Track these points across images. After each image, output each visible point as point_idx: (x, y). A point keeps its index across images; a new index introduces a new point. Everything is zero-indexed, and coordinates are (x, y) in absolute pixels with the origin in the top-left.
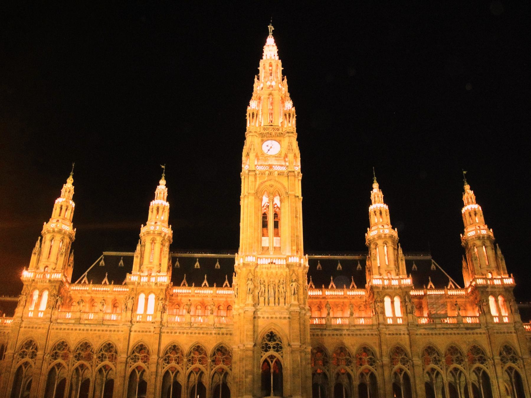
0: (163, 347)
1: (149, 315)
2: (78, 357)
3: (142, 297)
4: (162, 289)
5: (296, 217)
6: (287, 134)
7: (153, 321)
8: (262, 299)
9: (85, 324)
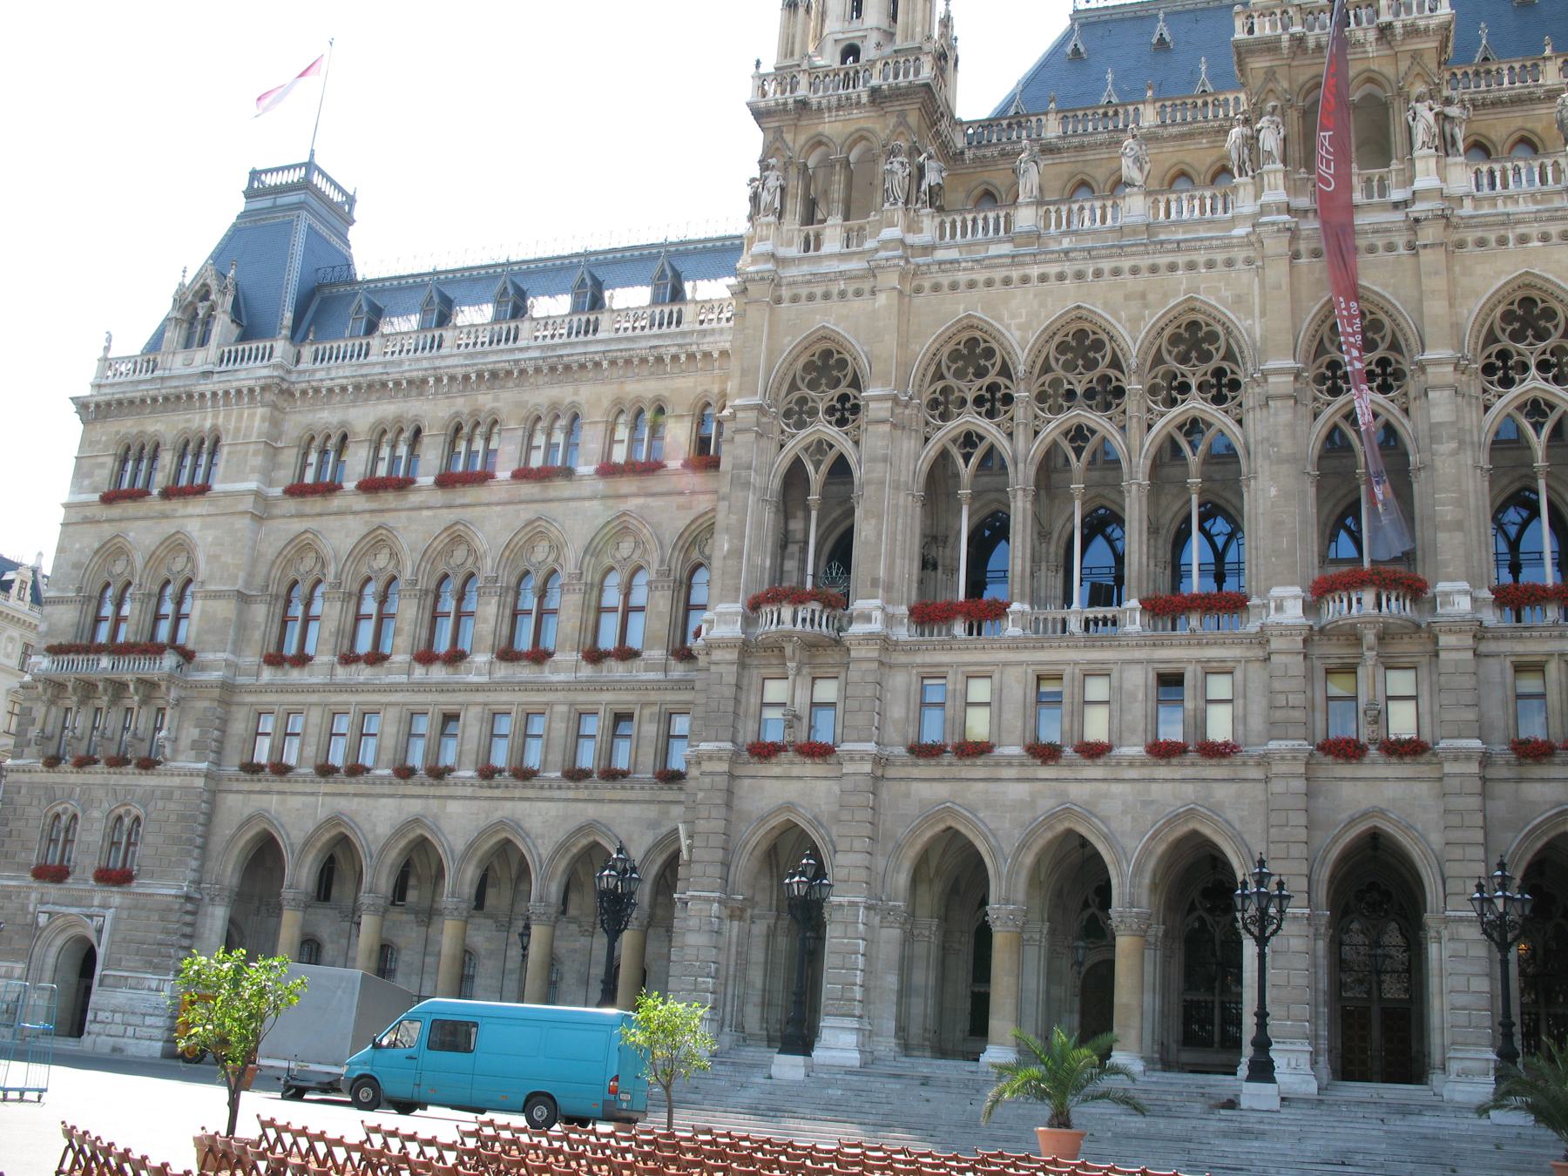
2: (1053, 398)
4: (1416, 56)
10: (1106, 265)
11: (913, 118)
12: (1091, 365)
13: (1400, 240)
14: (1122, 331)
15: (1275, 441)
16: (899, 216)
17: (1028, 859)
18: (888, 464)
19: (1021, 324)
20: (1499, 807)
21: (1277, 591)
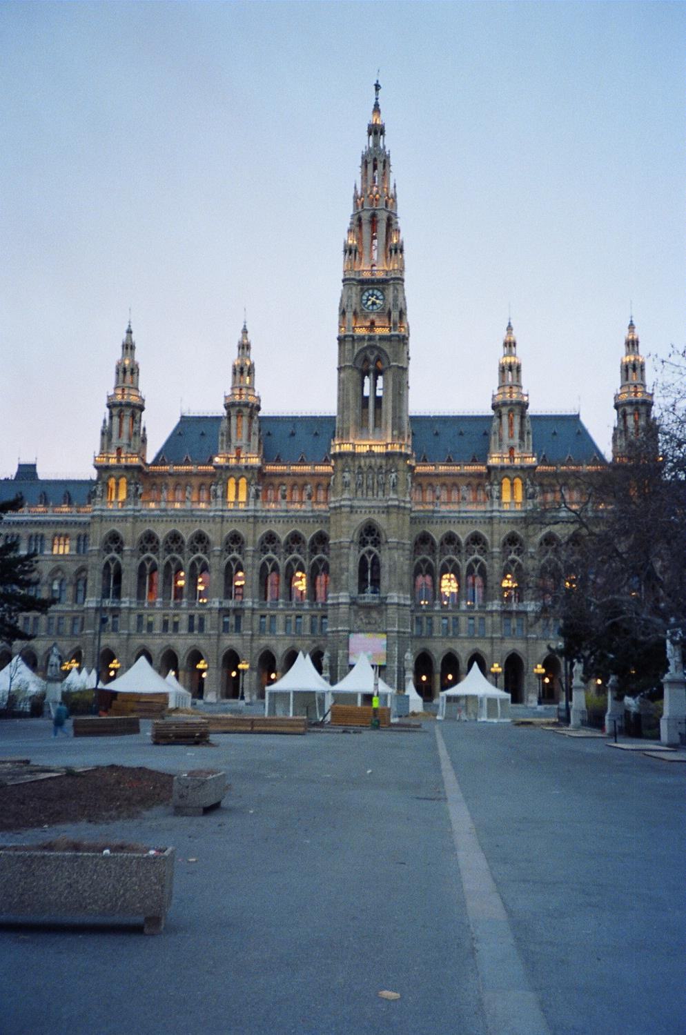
0: (258, 537)
1: (242, 502)
2: (169, 550)
3: (232, 482)
5: (400, 394)
6: (392, 282)
7: (246, 508)
8: (359, 493)
9: (172, 516)
10: (182, 519)
11: (136, 474)
12: (177, 543)
13: (245, 519)
14: (184, 535)
15: (216, 563)
16: (133, 503)
17: (161, 655)
18: (130, 565)
19: (161, 532)
20: (254, 645)
21: (214, 599)
